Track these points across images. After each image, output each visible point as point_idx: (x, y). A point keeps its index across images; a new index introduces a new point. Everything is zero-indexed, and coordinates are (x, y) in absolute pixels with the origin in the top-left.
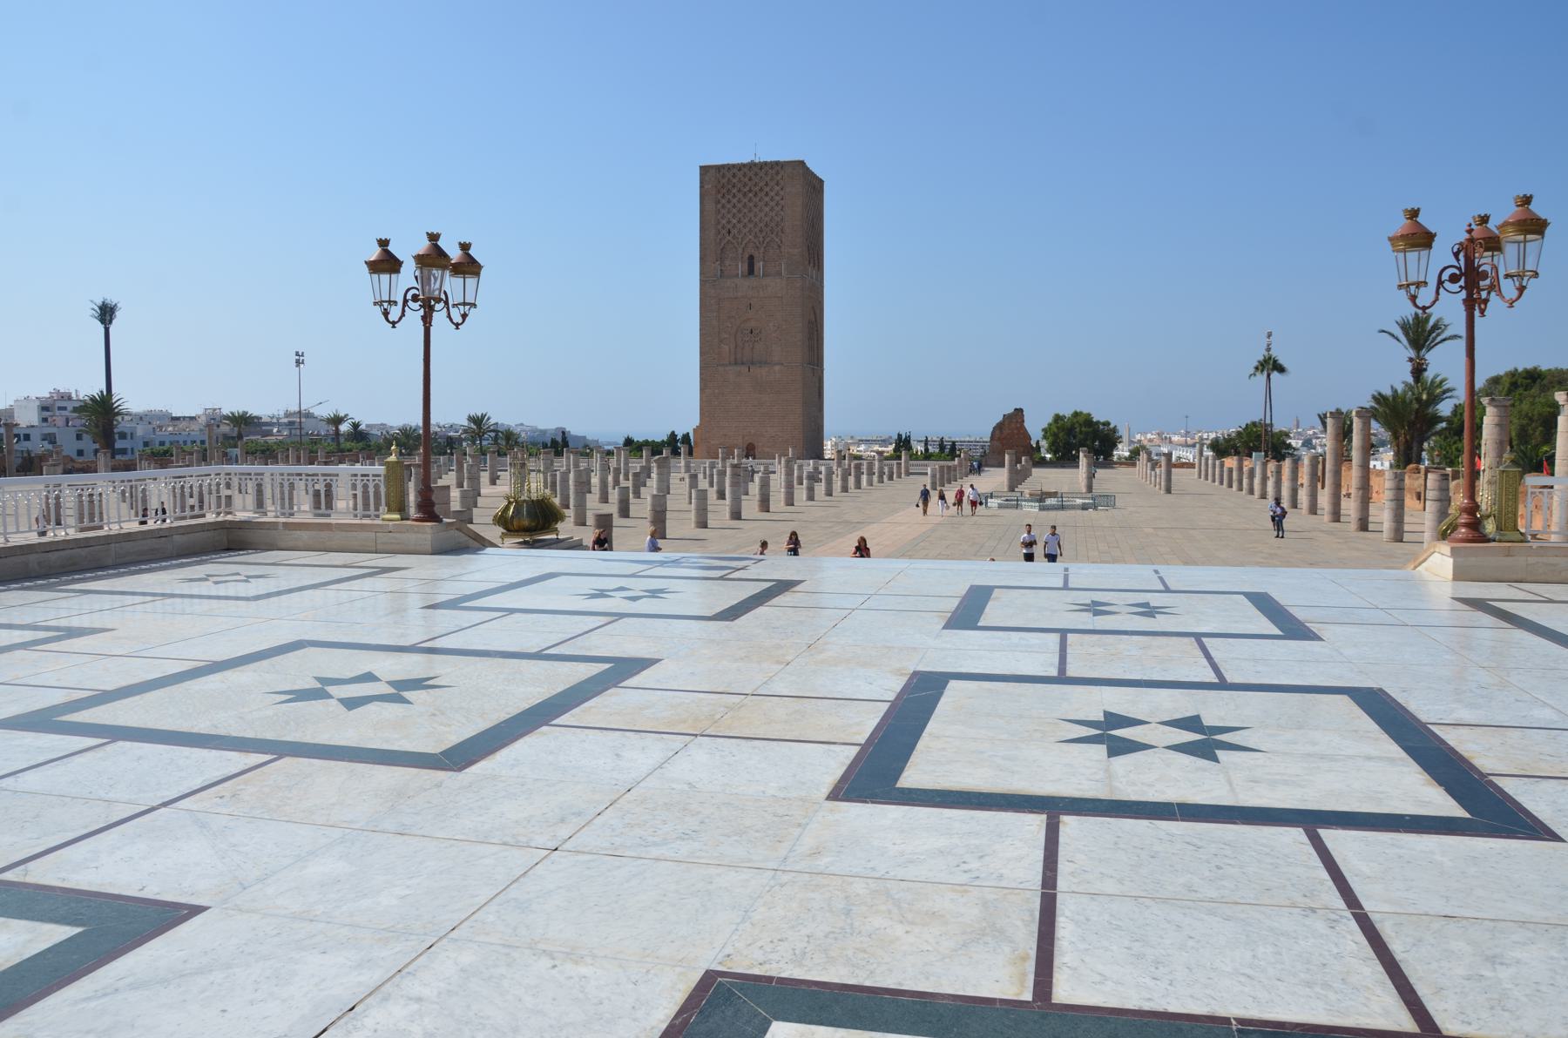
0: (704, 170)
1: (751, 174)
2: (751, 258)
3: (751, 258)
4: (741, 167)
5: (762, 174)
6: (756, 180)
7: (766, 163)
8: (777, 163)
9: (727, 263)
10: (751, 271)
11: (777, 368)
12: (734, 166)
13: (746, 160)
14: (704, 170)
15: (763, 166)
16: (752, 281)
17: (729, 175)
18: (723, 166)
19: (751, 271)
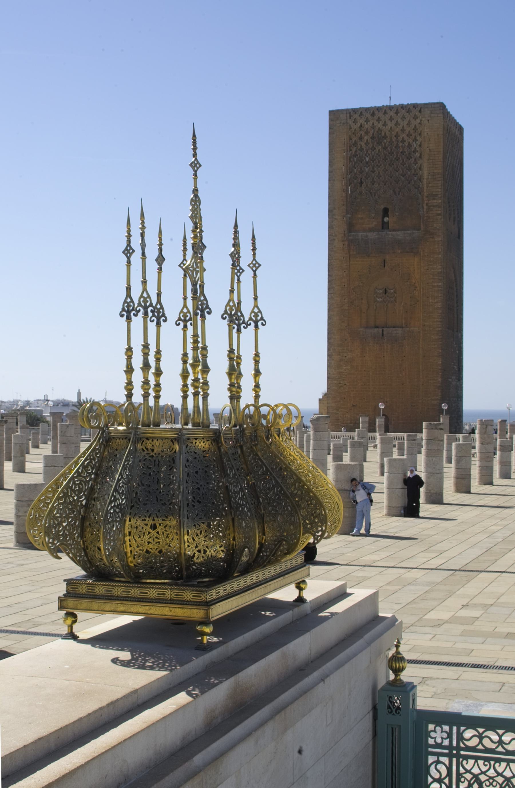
0: (334, 115)
8: (415, 106)
18: (355, 111)
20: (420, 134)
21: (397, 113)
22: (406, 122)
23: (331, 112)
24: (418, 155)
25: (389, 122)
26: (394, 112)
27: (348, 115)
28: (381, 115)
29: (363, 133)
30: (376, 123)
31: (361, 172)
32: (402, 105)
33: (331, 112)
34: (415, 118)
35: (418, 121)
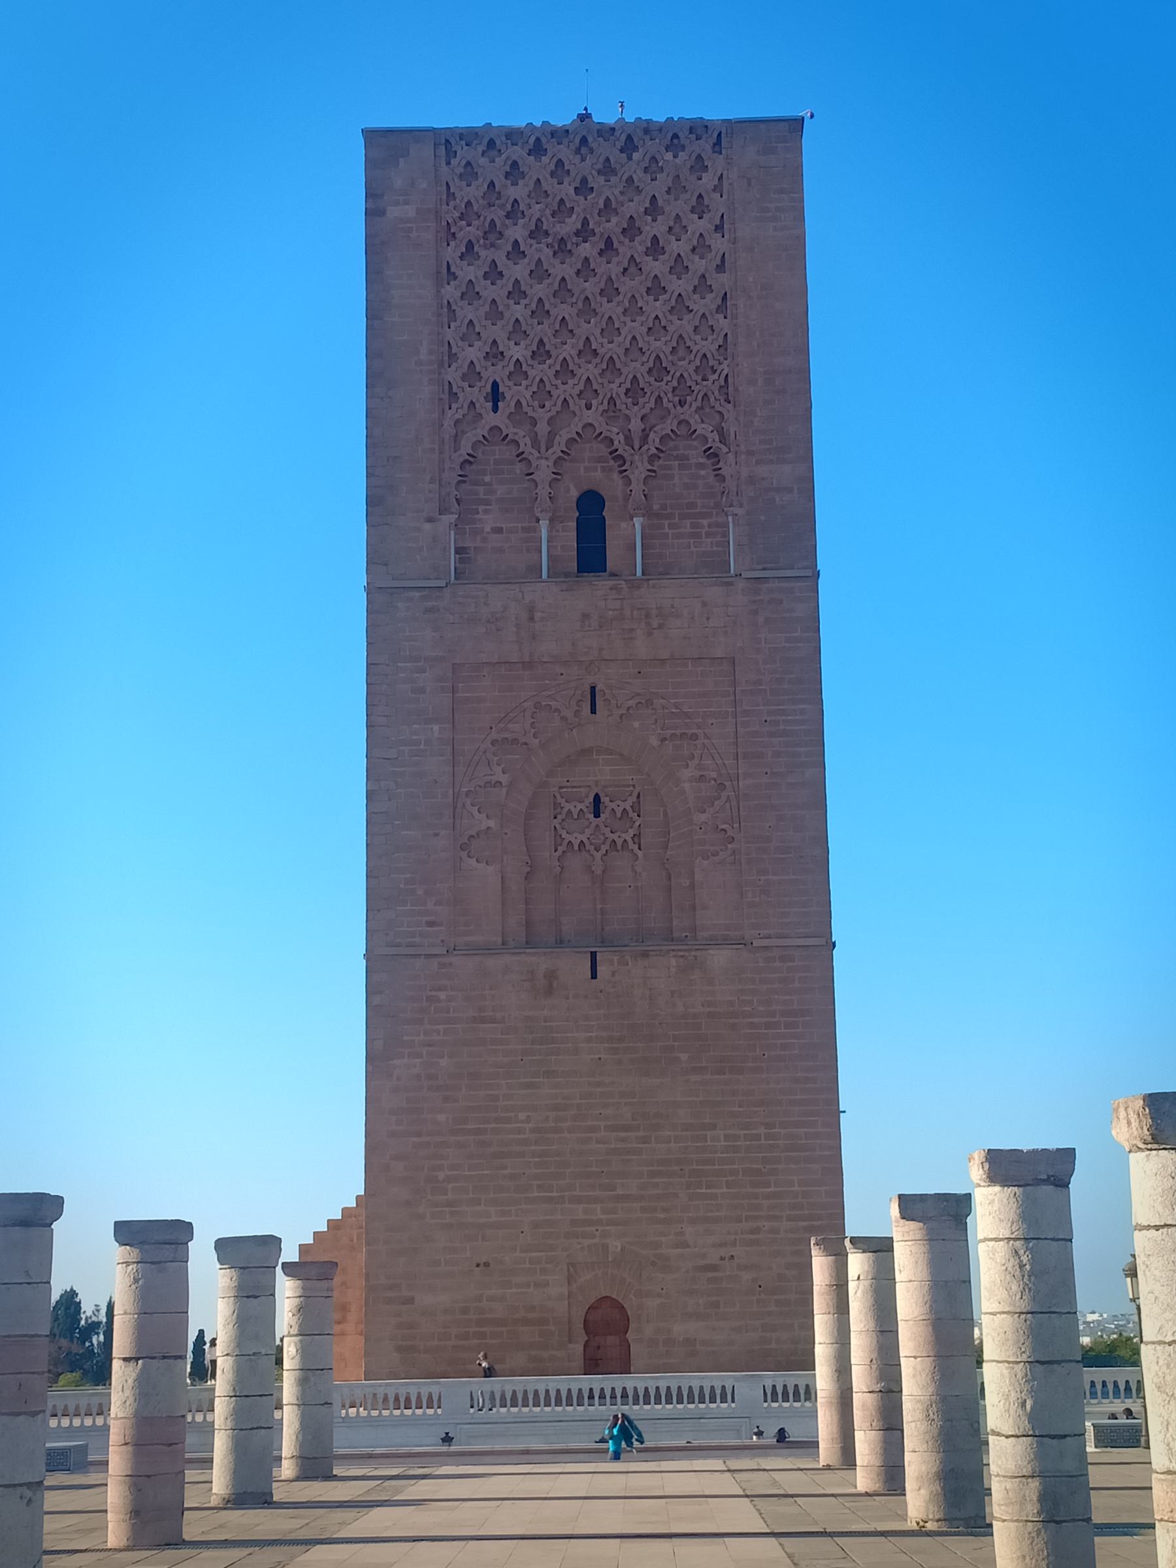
0: (385, 147)
1: (588, 167)
2: (591, 508)
3: (591, 508)
4: (539, 141)
5: (634, 168)
6: (610, 189)
7: (648, 128)
8: (698, 128)
9: (488, 520)
10: (591, 556)
11: (719, 958)
12: (512, 135)
13: (563, 118)
14: (385, 147)
15: (631, 138)
16: (596, 592)
17: (493, 169)
19: (591, 556)
20: (719, 228)
21: (629, 146)
22: (663, 181)
23: (372, 136)
24: (710, 302)
25: (597, 182)
26: (619, 145)
27: (442, 150)
28: (565, 152)
29: (497, 215)
30: (548, 184)
31: (495, 354)
32: (649, 121)
33: (372, 136)
34: (699, 165)
35: (708, 180)
